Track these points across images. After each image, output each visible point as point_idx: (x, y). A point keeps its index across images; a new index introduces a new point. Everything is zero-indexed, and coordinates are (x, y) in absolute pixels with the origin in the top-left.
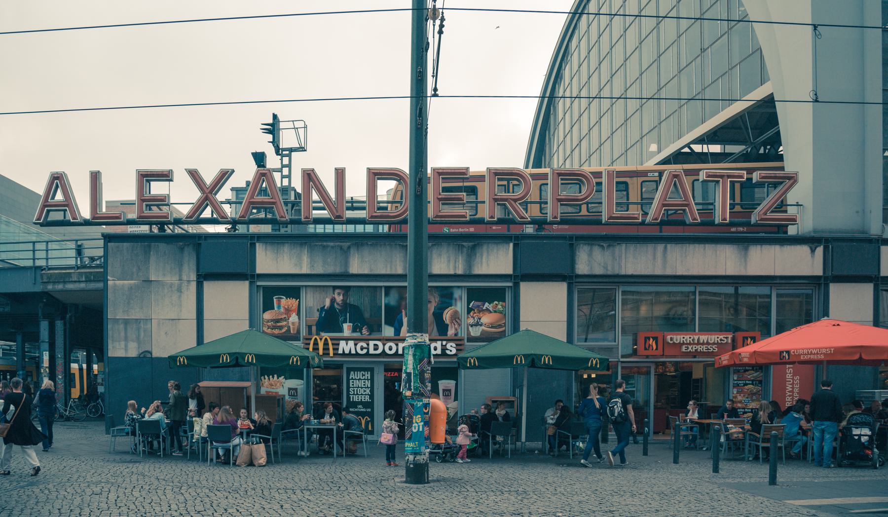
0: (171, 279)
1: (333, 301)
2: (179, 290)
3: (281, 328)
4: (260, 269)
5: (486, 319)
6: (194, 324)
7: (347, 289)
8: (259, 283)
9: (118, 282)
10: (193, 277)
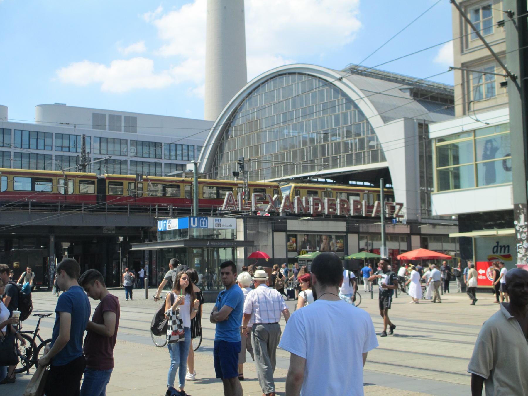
0: (265, 231)
1: (305, 239)
2: (267, 235)
3: (292, 247)
4: (289, 228)
5: (338, 245)
6: (271, 246)
7: (308, 235)
8: (288, 233)
9: (250, 232)
10: (271, 231)
